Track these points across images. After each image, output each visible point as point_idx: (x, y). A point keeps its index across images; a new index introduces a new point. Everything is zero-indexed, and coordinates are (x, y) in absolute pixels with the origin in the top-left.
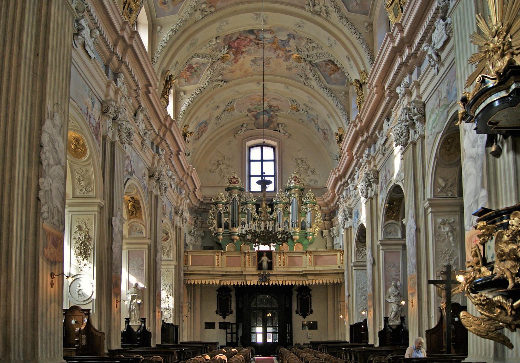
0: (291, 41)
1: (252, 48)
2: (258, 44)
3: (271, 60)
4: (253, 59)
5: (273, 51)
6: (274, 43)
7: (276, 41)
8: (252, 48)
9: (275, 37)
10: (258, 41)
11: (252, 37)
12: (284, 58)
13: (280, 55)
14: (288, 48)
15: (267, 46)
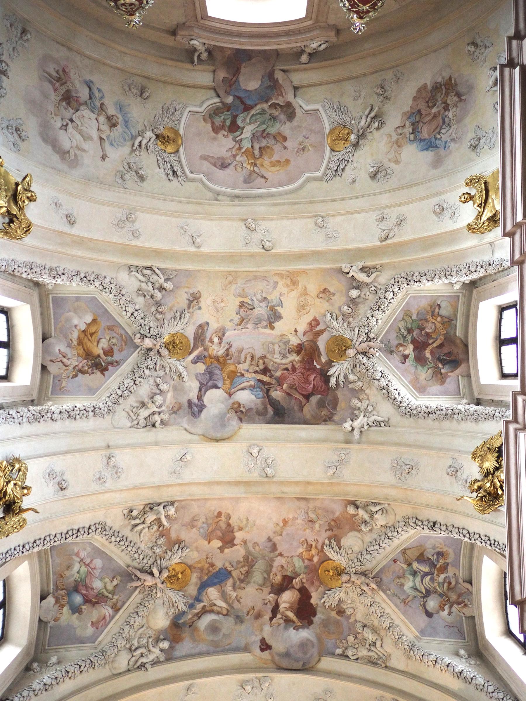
0: (196, 391)
1: (278, 360)
2: (265, 371)
3: (237, 319)
4: (277, 325)
5: (233, 350)
6: (233, 376)
7: (228, 382)
8: (277, 358)
9: (230, 395)
10: (266, 379)
11: (277, 394)
12: (208, 335)
13: (216, 340)
14: (201, 367)
15: (245, 366)
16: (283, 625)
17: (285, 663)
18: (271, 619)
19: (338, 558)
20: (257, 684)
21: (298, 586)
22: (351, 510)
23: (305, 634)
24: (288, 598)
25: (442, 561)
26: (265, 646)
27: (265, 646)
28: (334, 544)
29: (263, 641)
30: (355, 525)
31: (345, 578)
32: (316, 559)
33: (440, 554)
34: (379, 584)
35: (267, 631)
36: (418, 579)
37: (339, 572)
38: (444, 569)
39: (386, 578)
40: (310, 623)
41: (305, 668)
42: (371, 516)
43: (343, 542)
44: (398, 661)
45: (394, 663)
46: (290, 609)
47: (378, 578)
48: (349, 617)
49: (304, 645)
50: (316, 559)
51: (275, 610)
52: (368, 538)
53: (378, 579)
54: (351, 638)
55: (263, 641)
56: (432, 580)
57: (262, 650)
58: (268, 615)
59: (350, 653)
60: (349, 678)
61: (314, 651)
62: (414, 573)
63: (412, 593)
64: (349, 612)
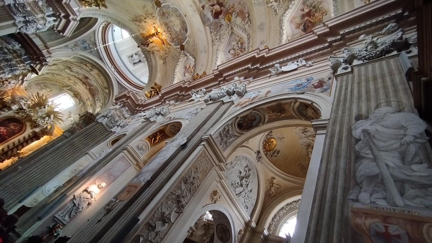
16: (210, 10)
17: (202, 16)
18: (210, 5)
19: (233, 18)
20: (194, 10)
21: (222, 9)
22: (247, 15)
23: (211, 18)
24: (217, 7)
25: (243, 50)
26: (203, 7)
27: (203, 7)
28: (236, 15)
29: (204, 6)
30: (243, 19)
31: (229, 23)
32: (230, 11)
33: (245, 49)
34: (231, 34)
35: (207, 6)
36: (237, 45)
37: (229, 20)
38: (242, 51)
39: (233, 36)
40: (214, 18)
41: (204, 23)
42: (247, 23)
43: (238, 17)
44: (215, 48)
45: (214, 46)
46: (215, 10)
47: (232, 33)
48: (220, 29)
49: (208, 19)
50: (230, 11)
51: (213, 5)
52: (241, 25)
53: (232, 33)
54: (216, 32)
55: (204, 6)
56: (238, 49)
57: (202, 7)
58: (210, 4)
59: (212, 34)
60: (207, 36)
61: (209, 24)
62: (237, 44)
63: (232, 45)
64: (221, 28)
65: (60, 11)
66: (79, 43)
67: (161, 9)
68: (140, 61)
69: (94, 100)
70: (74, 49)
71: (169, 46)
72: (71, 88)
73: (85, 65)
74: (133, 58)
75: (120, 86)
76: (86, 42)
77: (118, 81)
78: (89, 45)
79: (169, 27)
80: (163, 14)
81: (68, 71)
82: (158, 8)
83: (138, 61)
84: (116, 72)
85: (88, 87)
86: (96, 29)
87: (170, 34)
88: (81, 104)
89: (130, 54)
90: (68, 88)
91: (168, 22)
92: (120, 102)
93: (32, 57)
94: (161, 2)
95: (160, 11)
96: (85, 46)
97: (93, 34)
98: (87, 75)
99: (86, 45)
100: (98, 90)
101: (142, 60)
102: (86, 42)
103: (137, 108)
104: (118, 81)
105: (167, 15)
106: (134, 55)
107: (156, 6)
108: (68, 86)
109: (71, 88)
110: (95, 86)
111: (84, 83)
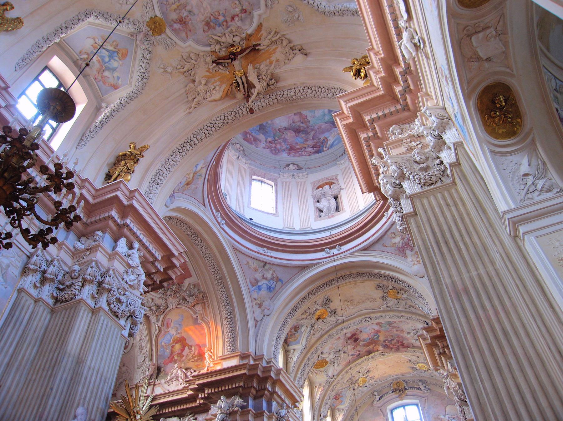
65: (107, 215)
66: (255, 295)
67: (171, 26)
68: (336, 198)
69: (414, 347)
70: (266, 312)
71: (263, 32)
72: (379, 392)
73: (318, 319)
74: (324, 210)
75: (377, 246)
76: (257, 281)
77: (365, 249)
78: (266, 279)
79: (216, 19)
80: (182, 21)
81: (332, 370)
82: (168, 31)
83: (333, 201)
84: (342, 247)
85: (381, 348)
86: (230, 243)
87: (233, 19)
88: (422, 388)
89: (312, 212)
90: (378, 397)
91: (203, 18)
92: (372, 156)
93: (253, 391)
94: (151, 14)
95: (175, 31)
96: (265, 286)
97: (241, 256)
98: (349, 335)
99: (262, 283)
100: (390, 324)
101: (334, 192)
102: (257, 281)
103: (398, 89)
104: (365, 249)
105: (185, 14)
106: (320, 206)
107: (163, 36)
108: (374, 395)
109: (379, 392)
110: (377, 328)
111: (369, 353)
